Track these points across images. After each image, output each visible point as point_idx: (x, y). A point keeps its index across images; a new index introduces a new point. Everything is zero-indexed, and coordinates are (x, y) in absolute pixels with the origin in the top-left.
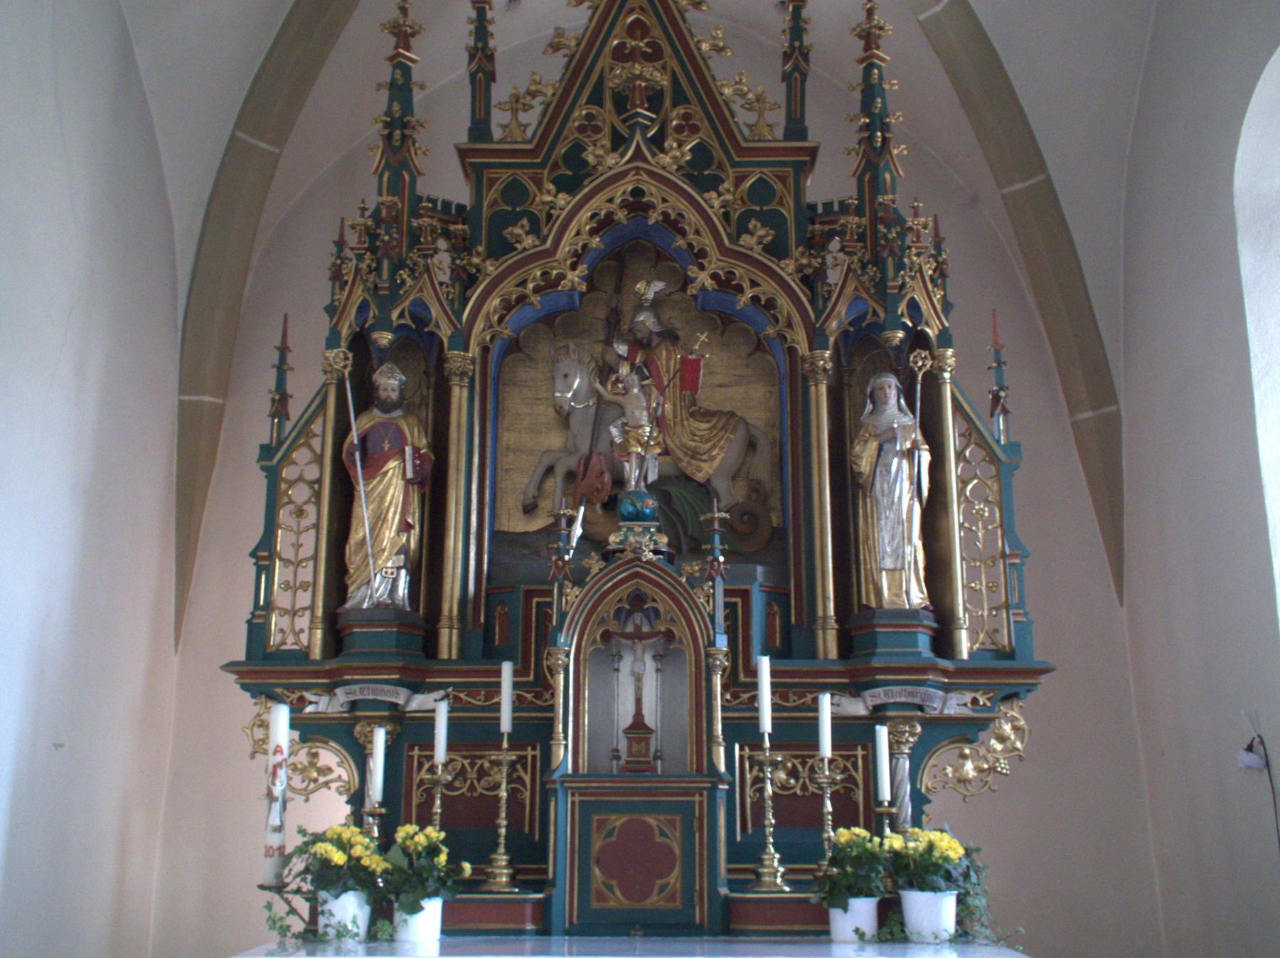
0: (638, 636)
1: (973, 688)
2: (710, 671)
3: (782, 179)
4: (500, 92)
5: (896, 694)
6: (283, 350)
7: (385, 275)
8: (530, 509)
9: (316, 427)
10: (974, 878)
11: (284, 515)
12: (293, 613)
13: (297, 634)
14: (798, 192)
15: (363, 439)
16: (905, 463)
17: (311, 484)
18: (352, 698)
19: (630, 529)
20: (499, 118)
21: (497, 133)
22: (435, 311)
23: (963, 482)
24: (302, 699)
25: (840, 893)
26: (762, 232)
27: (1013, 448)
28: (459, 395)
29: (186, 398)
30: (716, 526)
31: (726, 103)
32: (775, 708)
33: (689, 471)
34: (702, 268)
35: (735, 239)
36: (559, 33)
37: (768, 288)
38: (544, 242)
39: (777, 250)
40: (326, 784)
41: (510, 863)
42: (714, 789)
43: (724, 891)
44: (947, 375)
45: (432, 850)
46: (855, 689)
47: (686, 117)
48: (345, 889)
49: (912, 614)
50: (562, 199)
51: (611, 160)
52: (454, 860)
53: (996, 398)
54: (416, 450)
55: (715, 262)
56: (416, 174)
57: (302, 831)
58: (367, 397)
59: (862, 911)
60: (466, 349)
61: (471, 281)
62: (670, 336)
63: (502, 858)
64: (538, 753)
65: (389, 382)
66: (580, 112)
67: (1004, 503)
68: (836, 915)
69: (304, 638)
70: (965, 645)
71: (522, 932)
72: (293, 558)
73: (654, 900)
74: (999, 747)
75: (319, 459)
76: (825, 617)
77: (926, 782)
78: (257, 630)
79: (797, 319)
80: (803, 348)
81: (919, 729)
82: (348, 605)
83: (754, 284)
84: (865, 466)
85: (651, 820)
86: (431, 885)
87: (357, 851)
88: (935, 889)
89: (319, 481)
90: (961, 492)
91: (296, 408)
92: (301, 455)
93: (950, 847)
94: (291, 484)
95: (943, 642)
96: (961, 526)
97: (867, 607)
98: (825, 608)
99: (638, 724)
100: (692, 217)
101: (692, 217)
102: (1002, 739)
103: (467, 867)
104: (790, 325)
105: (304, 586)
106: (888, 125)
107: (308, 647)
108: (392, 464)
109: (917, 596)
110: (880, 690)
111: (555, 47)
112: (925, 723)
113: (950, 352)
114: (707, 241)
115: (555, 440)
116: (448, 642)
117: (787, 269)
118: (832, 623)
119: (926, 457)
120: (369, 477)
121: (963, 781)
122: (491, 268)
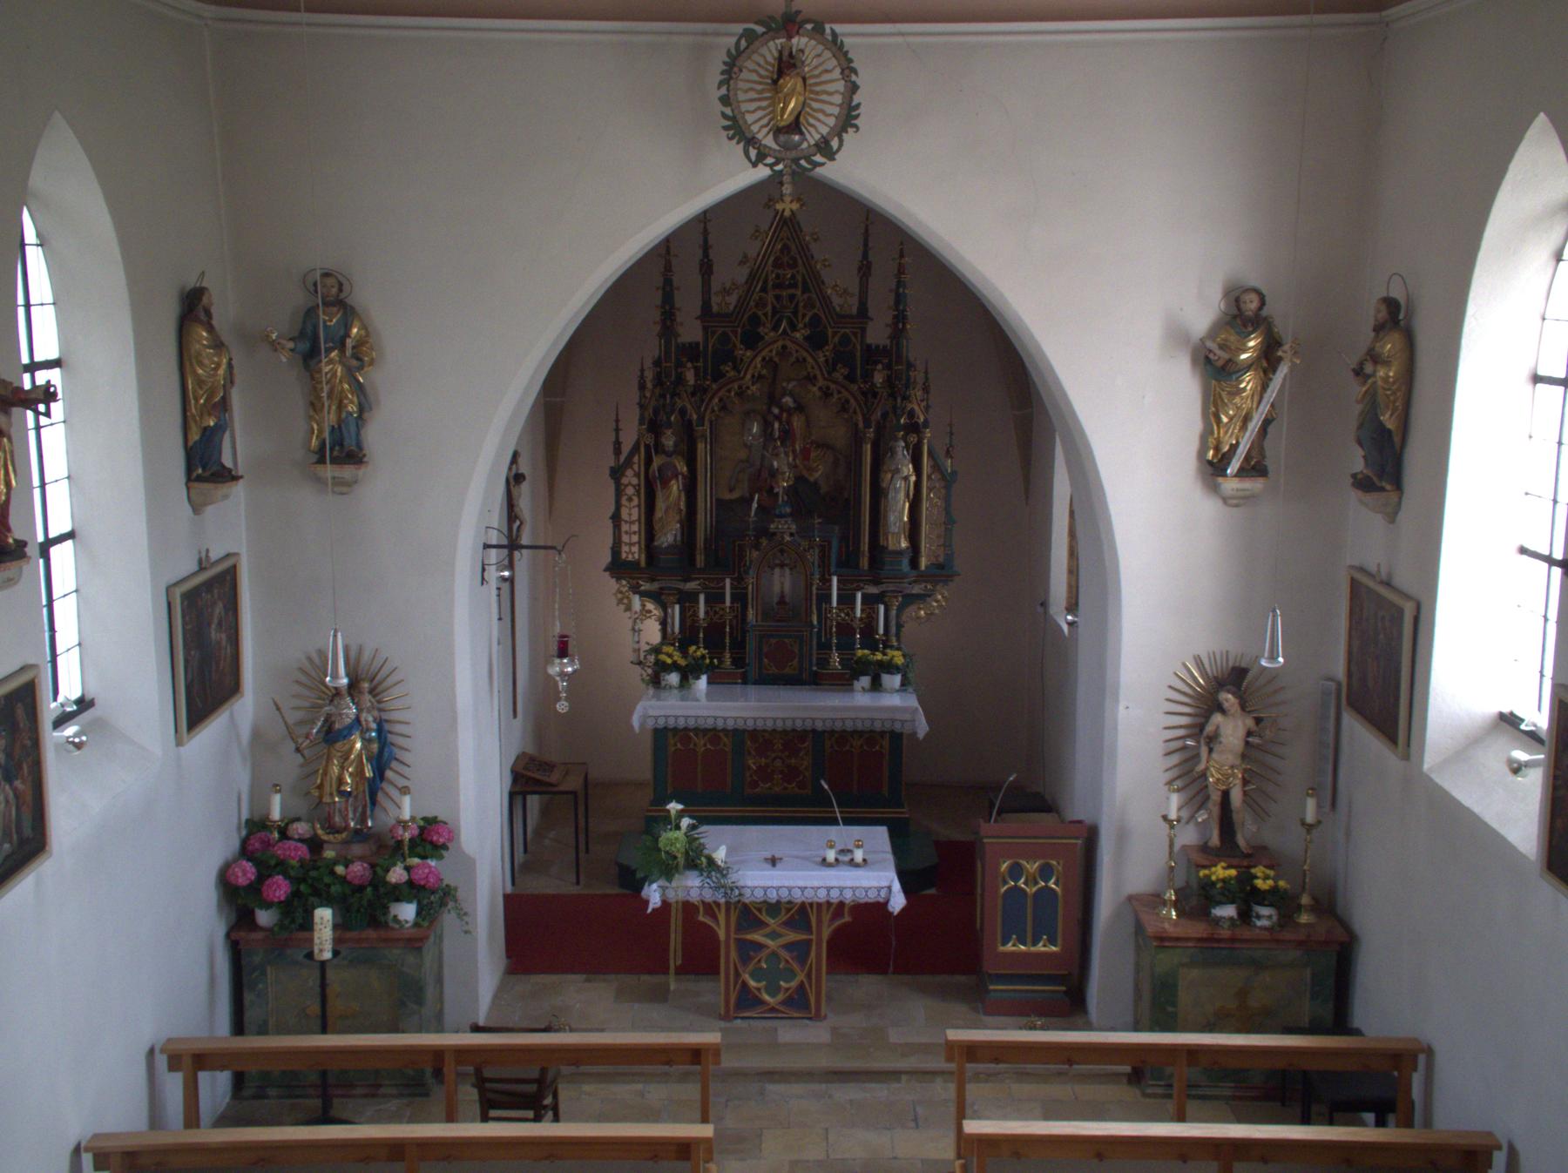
0: (782, 566)
1: (926, 582)
2: (812, 584)
3: (855, 334)
4: (715, 286)
5: (891, 587)
6: (617, 421)
7: (668, 401)
8: (731, 490)
9: (636, 459)
10: (910, 665)
11: (624, 501)
12: (631, 544)
13: (633, 554)
15: (660, 470)
16: (903, 483)
17: (634, 486)
18: (661, 585)
19: (779, 522)
20: (715, 300)
21: (715, 309)
22: (689, 407)
23: (930, 490)
24: (638, 583)
25: (856, 675)
26: (843, 370)
27: (954, 473)
28: (700, 446)
29: (548, 399)
30: (816, 526)
31: (829, 297)
32: (839, 589)
33: (806, 475)
34: (815, 385)
35: (829, 373)
36: (745, 256)
37: (845, 394)
38: (739, 372)
39: (851, 378)
40: (650, 617)
41: (731, 657)
42: (811, 631)
43: (815, 668)
44: (925, 441)
45: (703, 657)
46: (876, 583)
47: (809, 298)
48: (672, 672)
49: (900, 553)
50: (749, 353)
51: (772, 334)
52: (711, 659)
53: (948, 451)
54: (683, 475)
55: (821, 382)
56: (677, 335)
57: (648, 644)
58: (659, 448)
59: (865, 681)
60: (703, 425)
61: (705, 391)
62: (800, 408)
63: (728, 655)
64: (739, 605)
65: (669, 441)
66: (756, 296)
67: (947, 500)
68: (855, 682)
69: (636, 556)
70: (923, 563)
71: (736, 683)
72: (628, 519)
73: (787, 671)
74: (935, 604)
75: (637, 475)
76: (864, 551)
77: (904, 618)
78: (616, 552)
79: (858, 410)
80: (861, 425)
81: (900, 599)
82: (656, 543)
83: (839, 392)
84: (884, 485)
85: (786, 640)
86: (704, 670)
87: (675, 658)
88: (892, 673)
89: (639, 485)
90: (928, 494)
91: (626, 449)
92: (629, 473)
93: (899, 660)
94: (627, 486)
95: (914, 563)
96: (927, 509)
97: (883, 546)
98: (864, 547)
99: (782, 596)
100: (810, 359)
101: (810, 359)
102: (937, 601)
103: (715, 661)
104: (855, 412)
105: (635, 533)
106: (906, 315)
107: (639, 559)
108: (673, 482)
109: (904, 544)
110: (884, 585)
111: (742, 263)
112: (903, 597)
113: (928, 430)
114: (818, 373)
115: (743, 454)
116: (700, 560)
117: (854, 387)
118: (867, 554)
119: (913, 478)
120: (663, 488)
121: (919, 618)
122: (714, 386)
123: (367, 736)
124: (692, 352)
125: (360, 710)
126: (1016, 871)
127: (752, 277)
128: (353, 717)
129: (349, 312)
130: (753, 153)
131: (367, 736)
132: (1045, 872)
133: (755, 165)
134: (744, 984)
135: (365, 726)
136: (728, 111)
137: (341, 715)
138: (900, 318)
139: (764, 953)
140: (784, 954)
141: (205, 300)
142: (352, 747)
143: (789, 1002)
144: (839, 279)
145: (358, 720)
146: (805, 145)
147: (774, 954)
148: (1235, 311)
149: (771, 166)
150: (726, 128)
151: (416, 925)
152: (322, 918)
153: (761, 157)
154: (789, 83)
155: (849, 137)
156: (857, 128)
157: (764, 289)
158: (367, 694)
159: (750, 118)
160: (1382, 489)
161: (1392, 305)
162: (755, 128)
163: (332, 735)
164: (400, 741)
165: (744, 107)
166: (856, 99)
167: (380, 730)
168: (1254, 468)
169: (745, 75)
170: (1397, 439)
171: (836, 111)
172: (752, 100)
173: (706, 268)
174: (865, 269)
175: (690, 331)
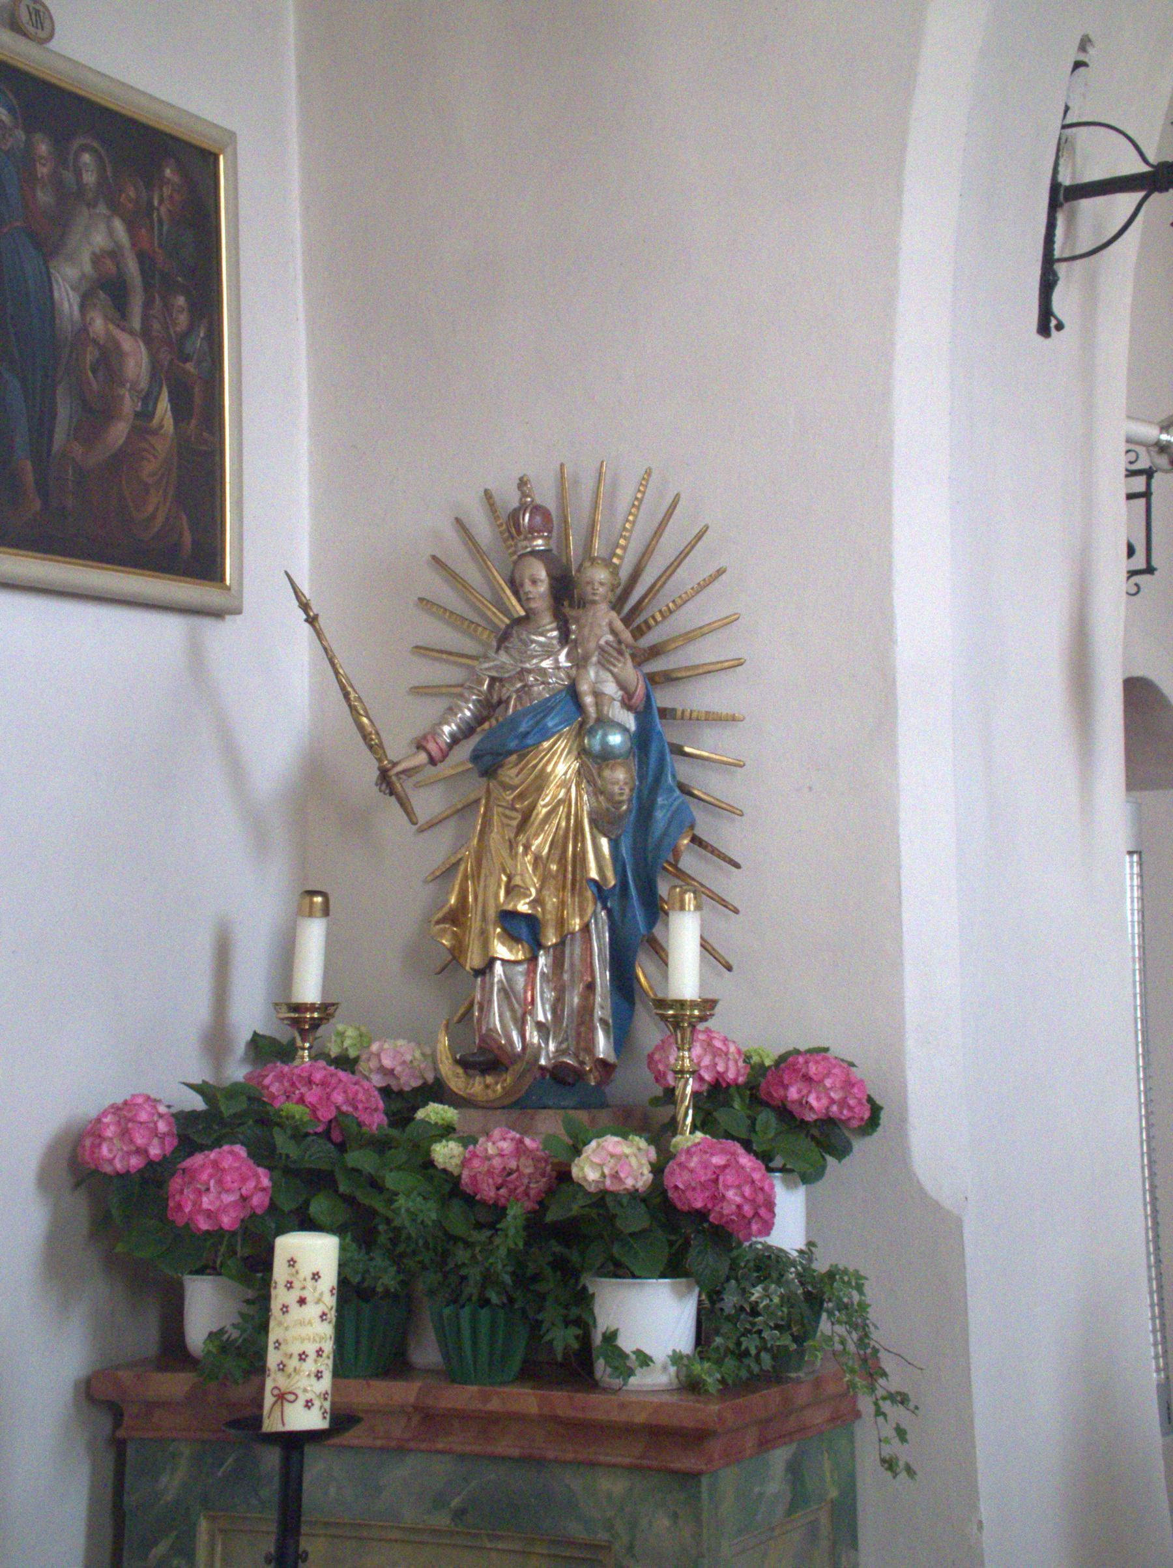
123: (595, 743)
125: (580, 662)
128: (558, 681)
131: (595, 743)
135: (592, 711)
137: (523, 672)
142: (541, 781)
151: (691, 1386)
152: (292, 1262)
158: (603, 607)
164: (708, 784)
167: (642, 740)
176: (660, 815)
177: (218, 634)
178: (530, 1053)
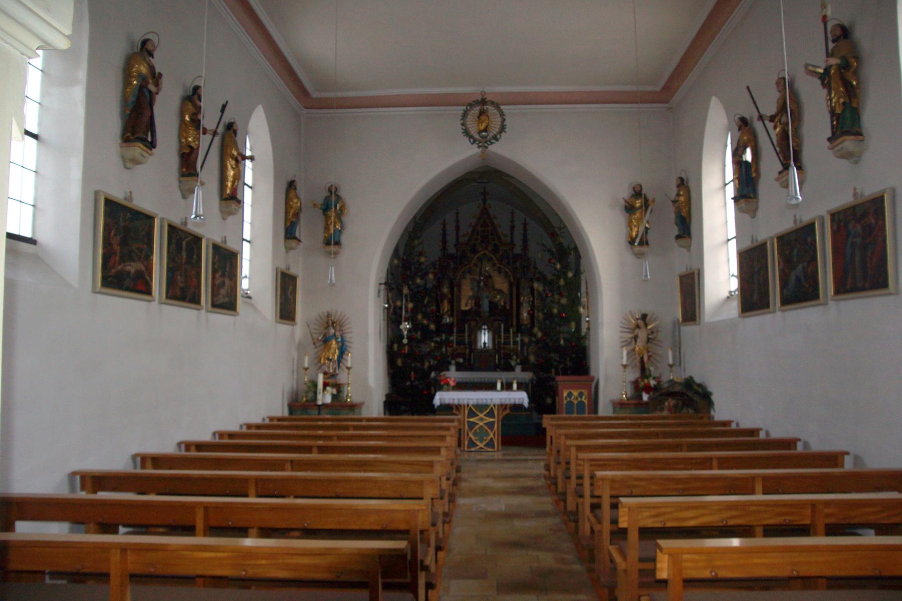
4: (461, 233)
8: (466, 305)
14: (512, 252)
20: (460, 239)
36: (471, 224)
39: (508, 263)
50: (472, 255)
55: (498, 265)
80: (512, 280)
124: (452, 257)
125: (335, 331)
126: (570, 395)
127: (473, 231)
129: (339, 198)
130: (472, 140)
132: (581, 395)
133: (472, 144)
134: (470, 438)
136: (464, 128)
138: (525, 241)
139: (477, 426)
140: (486, 428)
141: (294, 184)
143: (487, 445)
144: (504, 229)
145: (335, 335)
146: (488, 137)
147: (481, 426)
148: (633, 193)
149: (477, 144)
150: (463, 133)
153: (474, 141)
154: (483, 118)
155: (503, 134)
156: (505, 132)
157: (478, 235)
159: (470, 130)
160: (685, 237)
161: (682, 179)
162: (472, 132)
163: (326, 341)
165: (469, 126)
166: (505, 123)
167: (342, 339)
168: (644, 242)
169: (469, 117)
170: (687, 220)
171: (498, 127)
172: (471, 124)
173: (458, 228)
174: (512, 228)
175: (451, 250)
176: (344, 348)
177: (295, 327)
178: (330, 372)
